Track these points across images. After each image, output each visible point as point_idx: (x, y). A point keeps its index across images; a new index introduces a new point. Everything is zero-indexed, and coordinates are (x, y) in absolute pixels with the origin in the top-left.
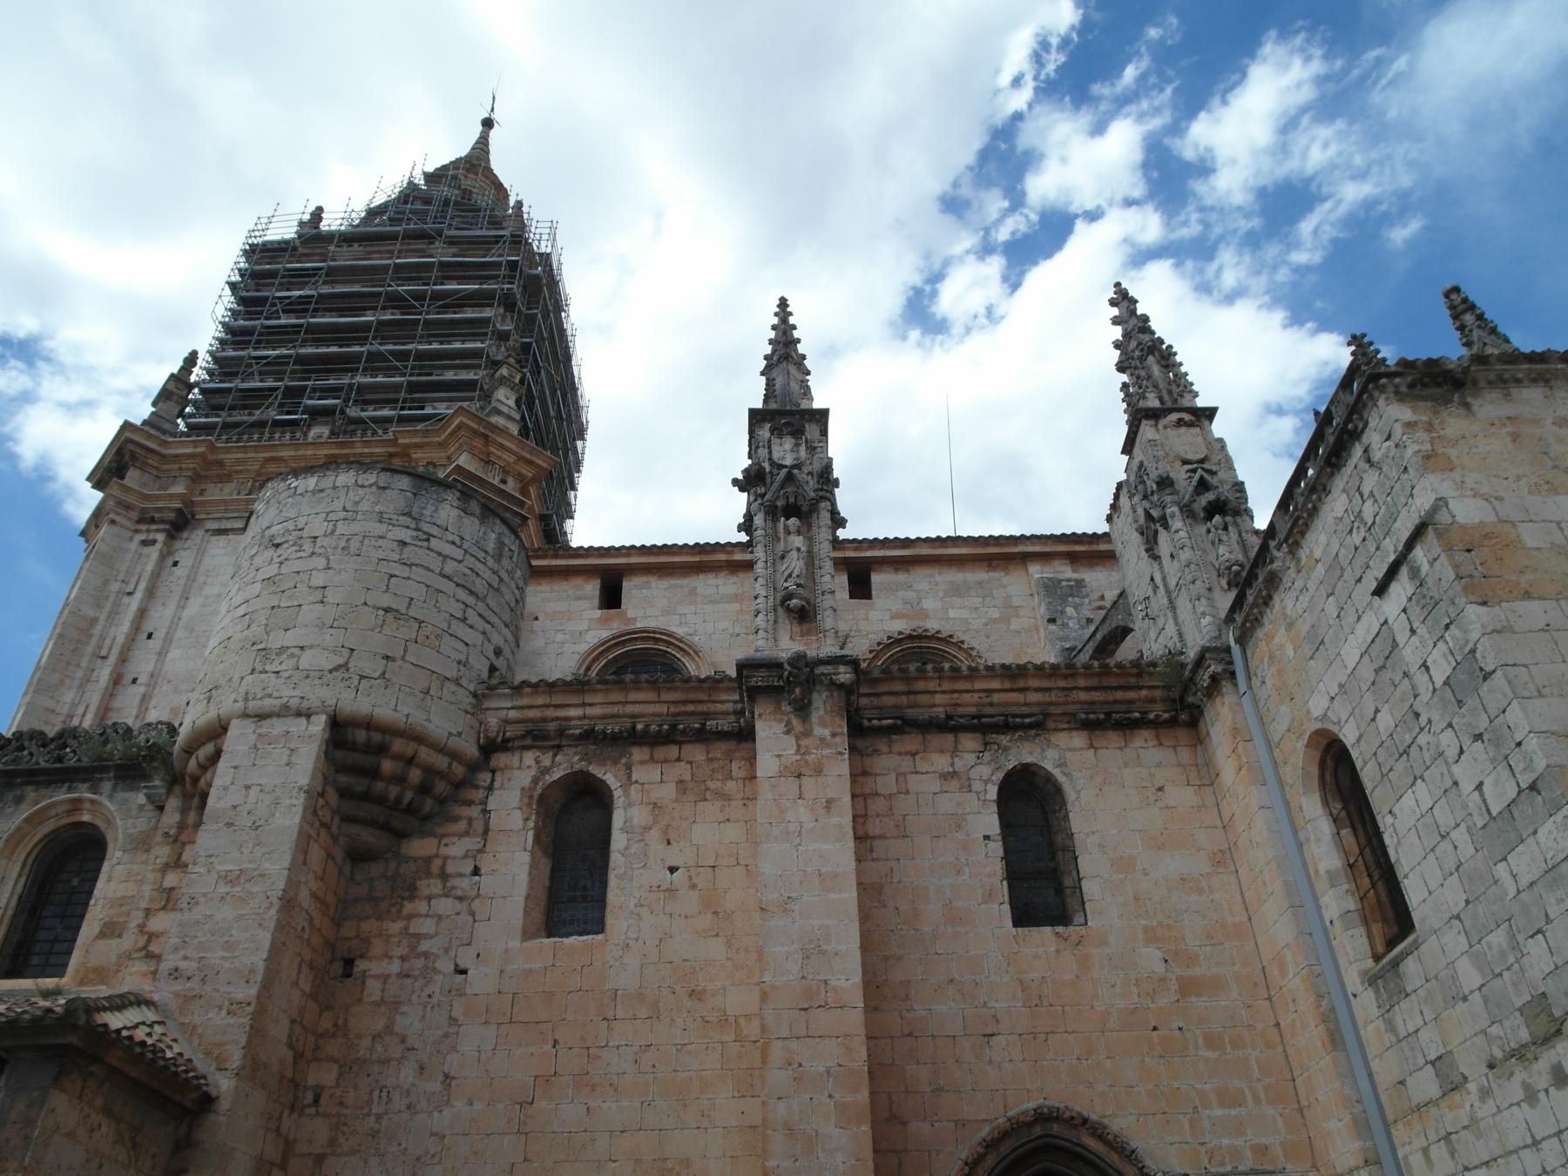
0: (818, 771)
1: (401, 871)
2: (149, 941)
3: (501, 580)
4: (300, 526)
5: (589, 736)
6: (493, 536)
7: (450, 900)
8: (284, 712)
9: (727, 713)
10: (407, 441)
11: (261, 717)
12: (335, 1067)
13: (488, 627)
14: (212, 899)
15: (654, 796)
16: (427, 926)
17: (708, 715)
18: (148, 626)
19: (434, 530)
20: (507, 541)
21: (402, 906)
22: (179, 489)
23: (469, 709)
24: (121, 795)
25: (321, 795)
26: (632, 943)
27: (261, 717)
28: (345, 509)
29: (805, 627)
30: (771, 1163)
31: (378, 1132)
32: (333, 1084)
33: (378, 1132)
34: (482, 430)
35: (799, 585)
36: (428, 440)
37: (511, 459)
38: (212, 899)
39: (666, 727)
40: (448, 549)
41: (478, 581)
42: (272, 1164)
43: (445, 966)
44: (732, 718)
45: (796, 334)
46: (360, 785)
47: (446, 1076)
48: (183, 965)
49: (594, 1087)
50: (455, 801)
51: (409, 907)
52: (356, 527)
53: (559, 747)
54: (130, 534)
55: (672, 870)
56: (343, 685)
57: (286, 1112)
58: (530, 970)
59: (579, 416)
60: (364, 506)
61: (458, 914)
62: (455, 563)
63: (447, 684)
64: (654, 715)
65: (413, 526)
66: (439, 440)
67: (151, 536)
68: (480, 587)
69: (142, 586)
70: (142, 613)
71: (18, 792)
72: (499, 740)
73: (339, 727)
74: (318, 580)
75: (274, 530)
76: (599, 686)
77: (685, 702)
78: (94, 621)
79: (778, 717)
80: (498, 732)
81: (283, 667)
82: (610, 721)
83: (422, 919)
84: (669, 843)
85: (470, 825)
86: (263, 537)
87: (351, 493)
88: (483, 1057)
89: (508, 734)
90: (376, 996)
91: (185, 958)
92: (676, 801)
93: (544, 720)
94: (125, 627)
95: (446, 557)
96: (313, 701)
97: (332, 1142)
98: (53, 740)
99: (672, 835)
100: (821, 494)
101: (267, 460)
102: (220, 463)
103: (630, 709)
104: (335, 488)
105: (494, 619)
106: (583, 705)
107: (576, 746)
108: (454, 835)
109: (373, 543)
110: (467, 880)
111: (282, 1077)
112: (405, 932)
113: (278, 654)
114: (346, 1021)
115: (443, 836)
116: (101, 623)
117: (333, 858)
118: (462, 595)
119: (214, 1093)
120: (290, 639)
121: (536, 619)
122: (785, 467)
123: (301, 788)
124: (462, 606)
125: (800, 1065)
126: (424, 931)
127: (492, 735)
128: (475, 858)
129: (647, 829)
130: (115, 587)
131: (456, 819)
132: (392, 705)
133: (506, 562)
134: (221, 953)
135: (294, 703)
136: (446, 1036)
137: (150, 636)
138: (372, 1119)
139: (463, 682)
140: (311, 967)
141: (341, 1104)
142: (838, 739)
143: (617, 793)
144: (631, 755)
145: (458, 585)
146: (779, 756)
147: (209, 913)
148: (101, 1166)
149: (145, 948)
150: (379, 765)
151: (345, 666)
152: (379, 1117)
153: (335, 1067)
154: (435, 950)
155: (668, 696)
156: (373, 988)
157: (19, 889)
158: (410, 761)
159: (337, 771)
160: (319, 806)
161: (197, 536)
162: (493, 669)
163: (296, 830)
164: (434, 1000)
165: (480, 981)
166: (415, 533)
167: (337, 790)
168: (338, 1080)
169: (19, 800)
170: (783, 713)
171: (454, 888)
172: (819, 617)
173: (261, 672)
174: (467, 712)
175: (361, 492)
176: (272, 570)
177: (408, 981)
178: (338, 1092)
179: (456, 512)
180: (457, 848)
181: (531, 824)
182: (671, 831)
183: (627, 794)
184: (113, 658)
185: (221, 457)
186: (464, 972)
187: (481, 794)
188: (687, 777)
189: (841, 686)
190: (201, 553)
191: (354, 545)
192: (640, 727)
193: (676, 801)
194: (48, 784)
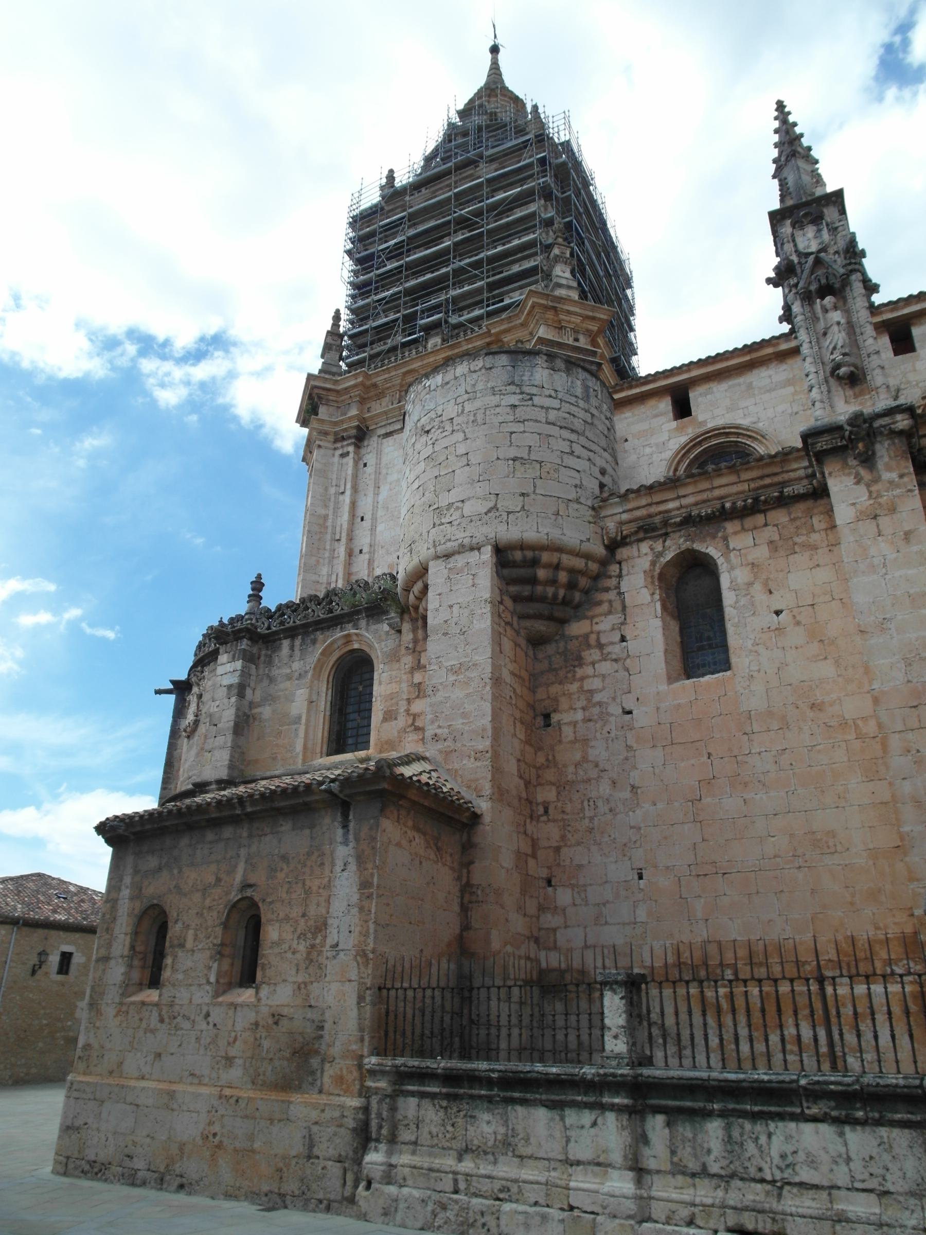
0: (892, 510)
1: (569, 647)
2: (414, 720)
3: (593, 415)
4: (439, 414)
5: (688, 521)
6: (579, 383)
7: (608, 663)
8: (462, 549)
9: (800, 479)
10: (497, 330)
11: (447, 556)
12: (554, 788)
13: (591, 454)
14: (447, 686)
15: (750, 558)
16: (596, 683)
17: (783, 484)
18: (360, 513)
19: (534, 390)
20: (590, 384)
21: (575, 672)
22: (354, 412)
23: (591, 519)
24: (373, 627)
25: (501, 603)
26: (755, 674)
27: (447, 556)
28: (467, 392)
29: (857, 389)
30: (906, 829)
31: (593, 829)
32: (555, 799)
33: (593, 829)
34: (550, 304)
35: (844, 355)
36: (513, 324)
37: (578, 320)
38: (447, 686)
39: (750, 501)
40: (548, 402)
41: (575, 420)
42: (527, 855)
43: (616, 710)
44: (805, 482)
45: (798, 130)
46: (526, 590)
47: (633, 787)
48: (439, 731)
49: (746, 784)
50: (597, 590)
51: (580, 672)
52: (478, 404)
53: (666, 534)
54: (332, 452)
55: (778, 613)
56: (497, 521)
57: (528, 821)
58: (679, 705)
59: (623, 269)
60: (480, 386)
61: (617, 671)
62: (556, 412)
63: (571, 504)
64: (737, 493)
65: (518, 391)
66: (520, 321)
67: (345, 450)
68: (578, 424)
69: (349, 486)
70: (353, 504)
71: (312, 637)
72: (619, 538)
73: (501, 552)
74: (461, 450)
75: (423, 421)
76: (688, 480)
77: (761, 478)
78: (326, 517)
79: (847, 471)
80: (617, 533)
81: (454, 518)
82: (703, 505)
83: (591, 679)
84: (771, 592)
85: (611, 606)
86: (416, 428)
87: (468, 379)
88: (657, 771)
89: (624, 533)
90: (571, 737)
91: (439, 727)
92: (770, 558)
93: (650, 516)
94: (345, 517)
95: (547, 409)
96: (479, 538)
97: (563, 838)
98: (323, 599)
99: (772, 585)
100: (850, 268)
101: (405, 374)
102: (375, 385)
103: (717, 493)
104: (456, 378)
105: (594, 447)
106: (679, 497)
107: (680, 531)
108: (601, 615)
109: (493, 411)
110: (617, 646)
111: (520, 799)
112: (581, 689)
113: (448, 510)
114: (554, 756)
115: (592, 618)
116: (331, 517)
117: (520, 646)
118: (566, 434)
119: (479, 812)
120: (453, 497)
121: (626, 440)
122: (812, 253)
123: (486, 601)
124: (569, 443)
125: (918, 751)
126: (595, 687)
127: (613, 535)
128: (620, 629)
129: (750, 584)
130: (332, 490)
131: (600, 603)
132: (535, 528)
133: (593, 401)
134: (461, 721)
135: (467, 541)
136: (627, 759)
137: (362, 519)
138: (587, 821)
139: (582, 500)
140: (522, 723)
141: (563, 812)
142: (906, 479)
143: (720, 561)
144: (725, 529)
145: (561, 428)
146: (854, 504)
147: (447, 695)
148: (421, 863)
149: (413, 724)
150: (535, 574)
151: (495, 508)
152: (591, 819)
153: (554, 788)
154: (605, 700)
155: (746, 476)
156: (568, 733)
157: (329, 698)
158: (557, 567)
159: (507, 584)
160: (501, 611)
161: (373, 442)
162: (602, 486)
163: (490, 630)
164: (613, 735)
165: (643, 717)
166: (521, 396)
167: (511, 597)
168: (557, 796)
169: (314, 642)
170: (850, 467)
171: (609, 653)
172: (869, 378)
173: (439, 525)
174: (590, 523)
175: (475, 376)
176: (428, 451)
177: (591, 724)
178: (559, 805)
179: (547, 371)
180: (605, 624)
181: (657, 597)
182: (770, 583)
183: (728, 560)
184: (344, 540)
185: (374, 380)
186: (630, 712)
187: (613, 582)
188: (776, 537)
189: (901, 433)
190: (379, 453)
191: (480, 417)
192: (728, 505)
193: (770, 558)
194: (329, 628)
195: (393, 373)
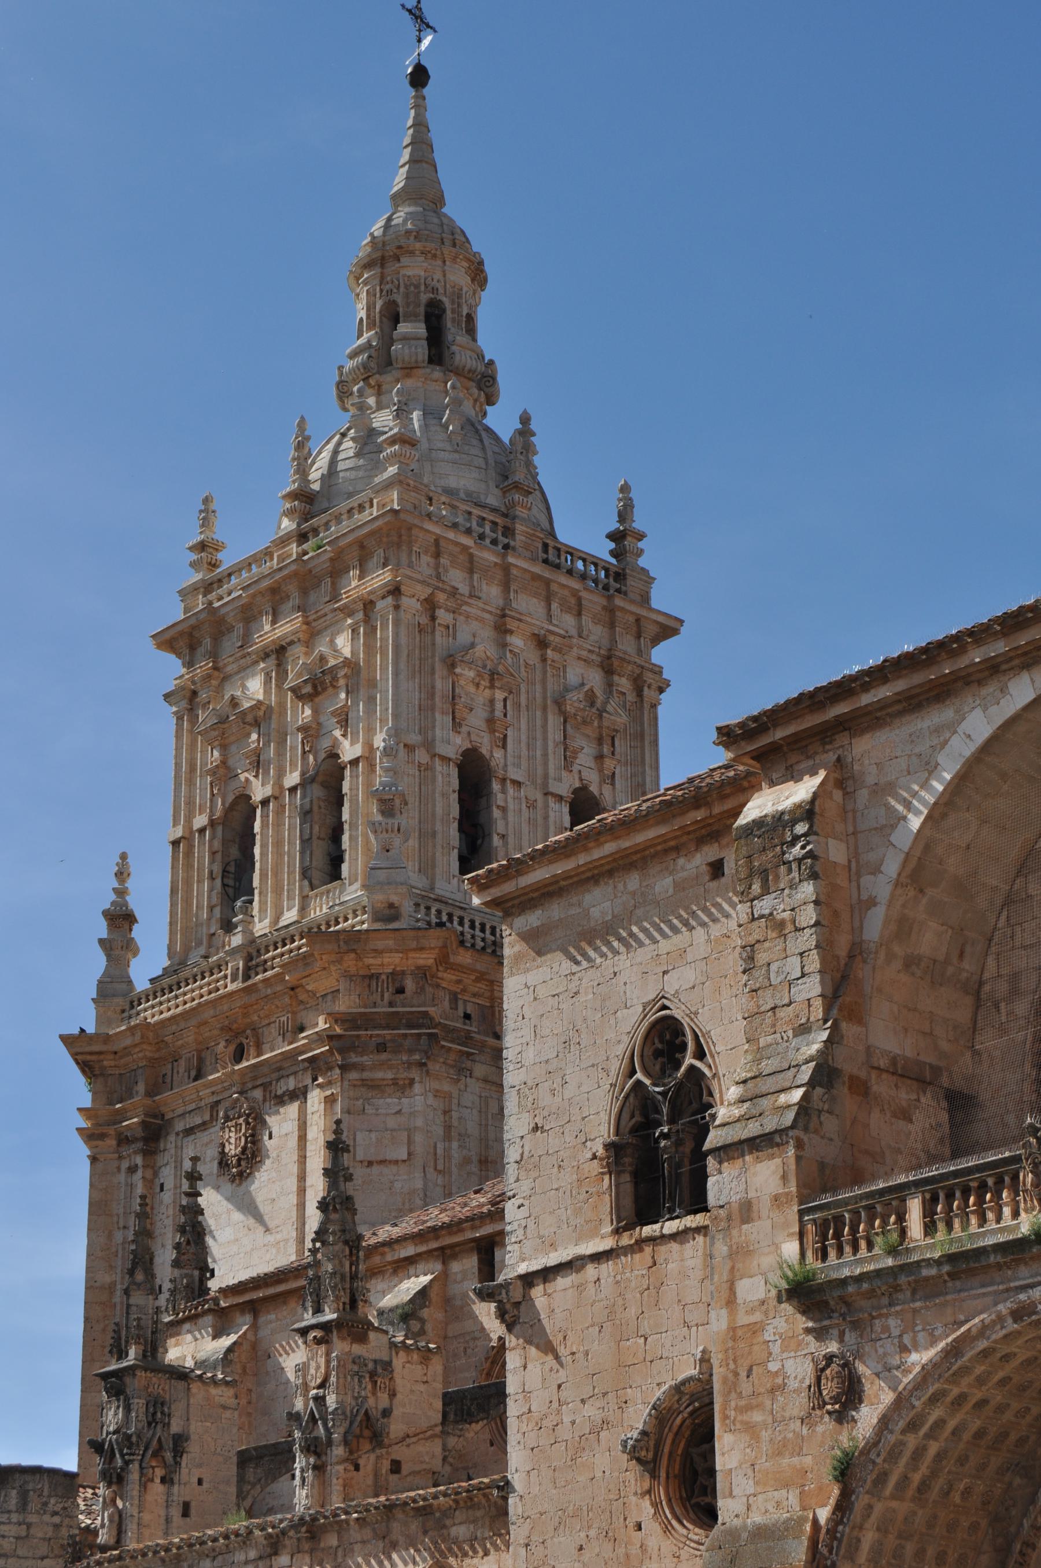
3: (29, 1526)
20: (30, 1486)
121: (269, 1357)
133: (34, 1504)
195: (182, 1025)
